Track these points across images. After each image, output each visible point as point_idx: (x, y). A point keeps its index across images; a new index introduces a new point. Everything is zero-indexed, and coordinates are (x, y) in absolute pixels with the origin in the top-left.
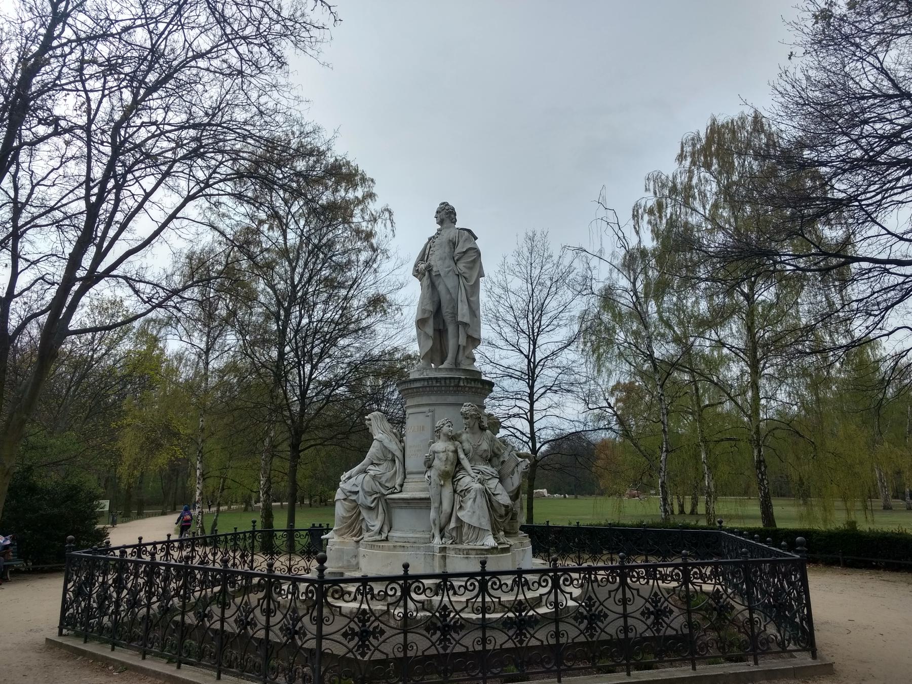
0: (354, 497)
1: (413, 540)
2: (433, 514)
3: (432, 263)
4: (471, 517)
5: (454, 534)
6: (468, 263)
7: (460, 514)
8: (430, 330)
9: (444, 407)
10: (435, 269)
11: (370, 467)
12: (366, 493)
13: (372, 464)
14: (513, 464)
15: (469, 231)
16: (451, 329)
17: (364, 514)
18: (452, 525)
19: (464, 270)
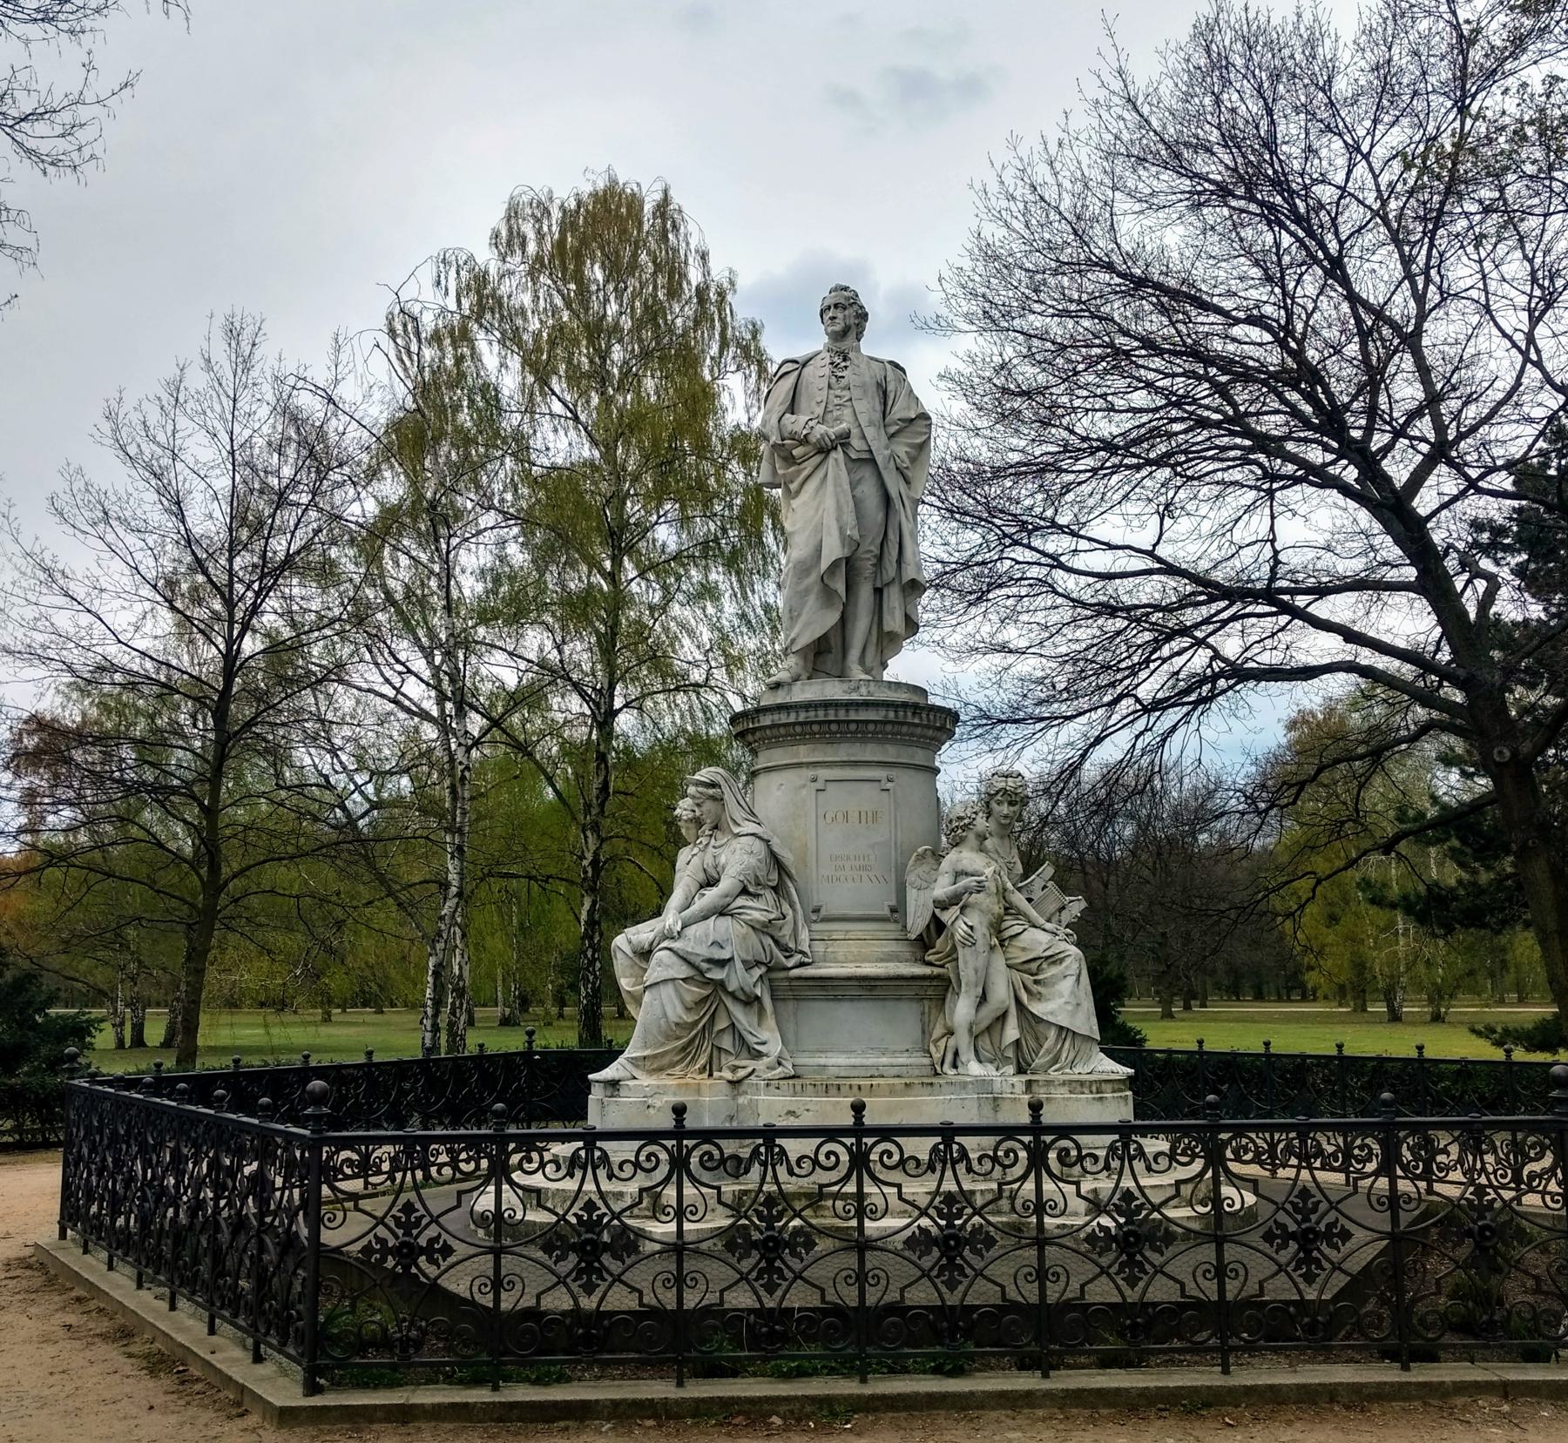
0: (717, 974)
1: (895, 1071)
2: (962, 1009)
3: (855, 431)
4: (1073, 1014)
5: (1010, 1053)
6: (909, 445)
7: (1037, 1008)
8: (840, 587)
9: (912, 772)
10: (856, 442)
11: (741, 901)
12: (744, 962)
13: (744, 891)
14: (1053, 907)
15: (903, 370)
16: (865, 594)
17: (738, 1012)
18: (1012, 1032)
19: (907, 463)
